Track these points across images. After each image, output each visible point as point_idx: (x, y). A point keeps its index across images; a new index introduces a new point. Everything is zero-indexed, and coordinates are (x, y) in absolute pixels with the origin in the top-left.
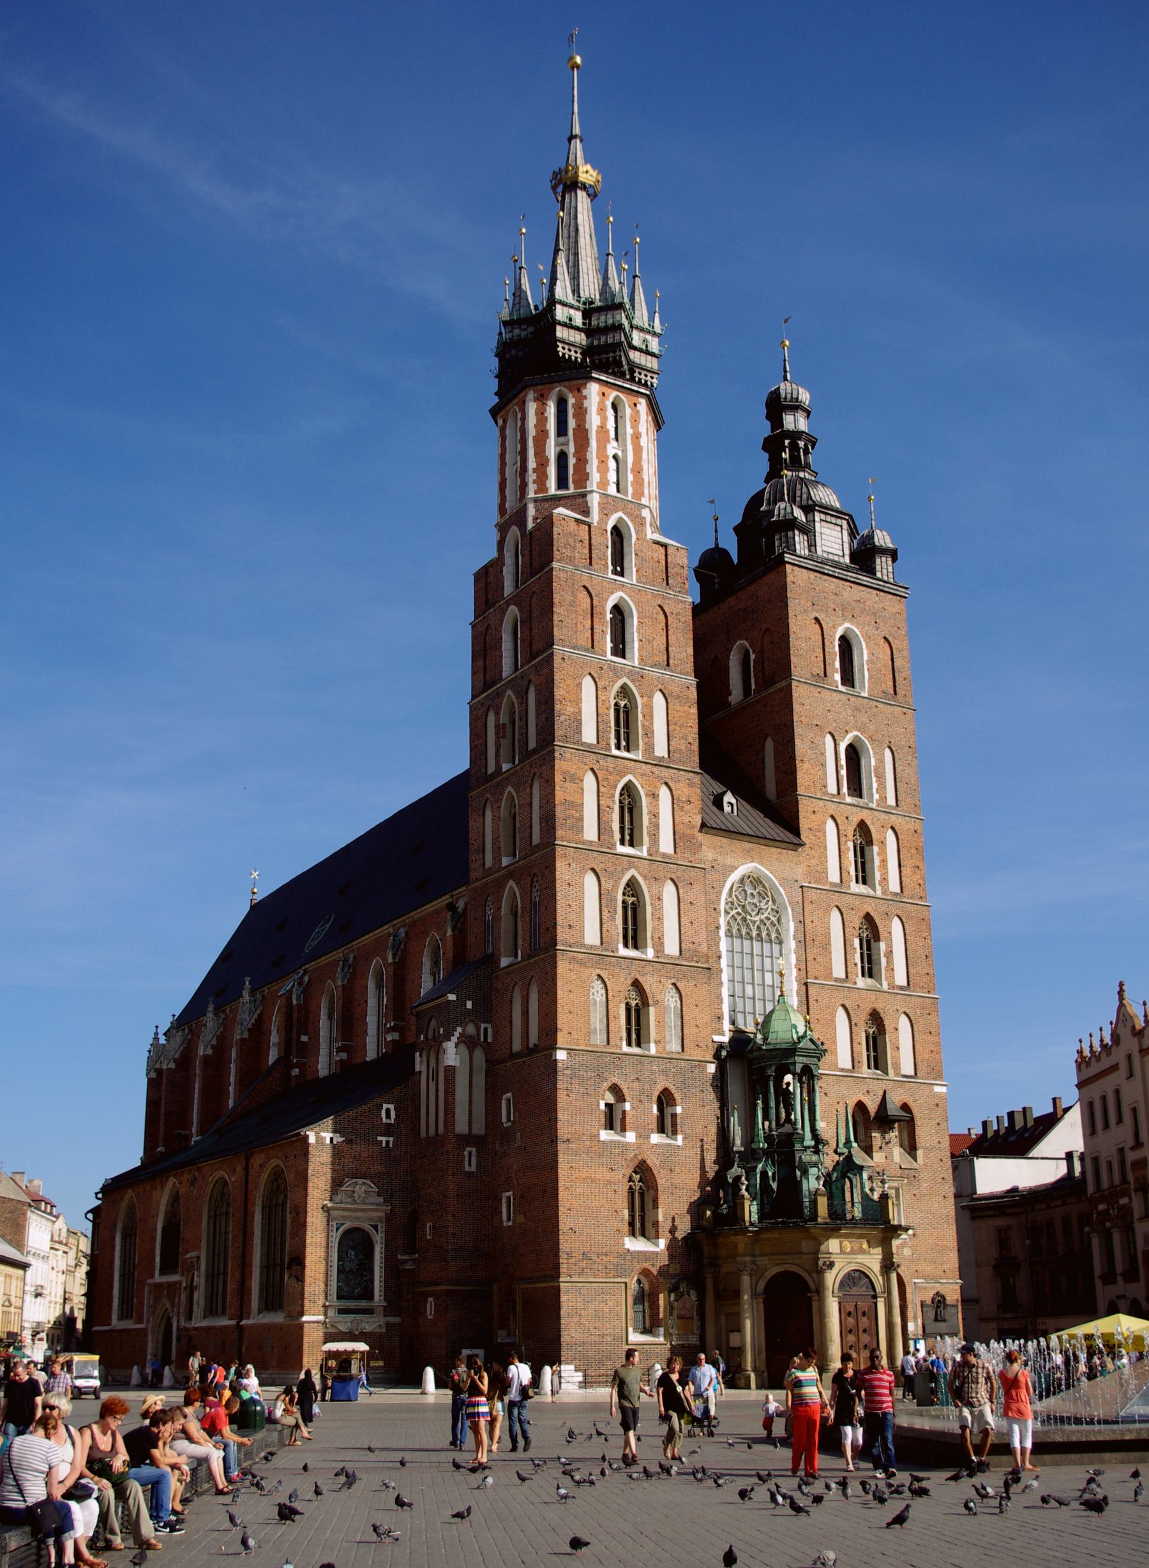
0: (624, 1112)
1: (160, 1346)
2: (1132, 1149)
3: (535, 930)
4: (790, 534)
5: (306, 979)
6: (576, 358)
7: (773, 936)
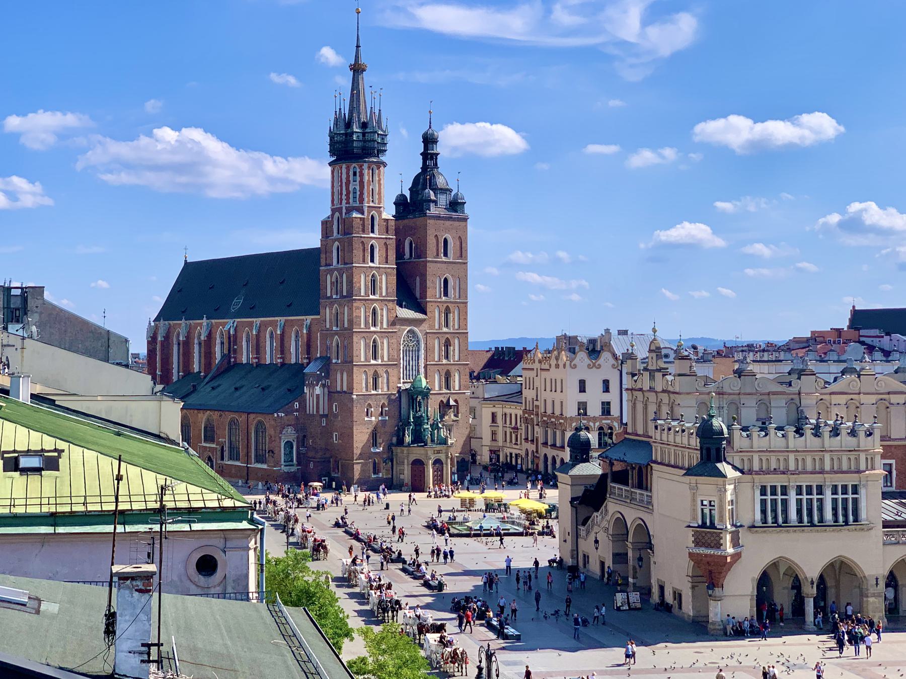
5: (235, 325)
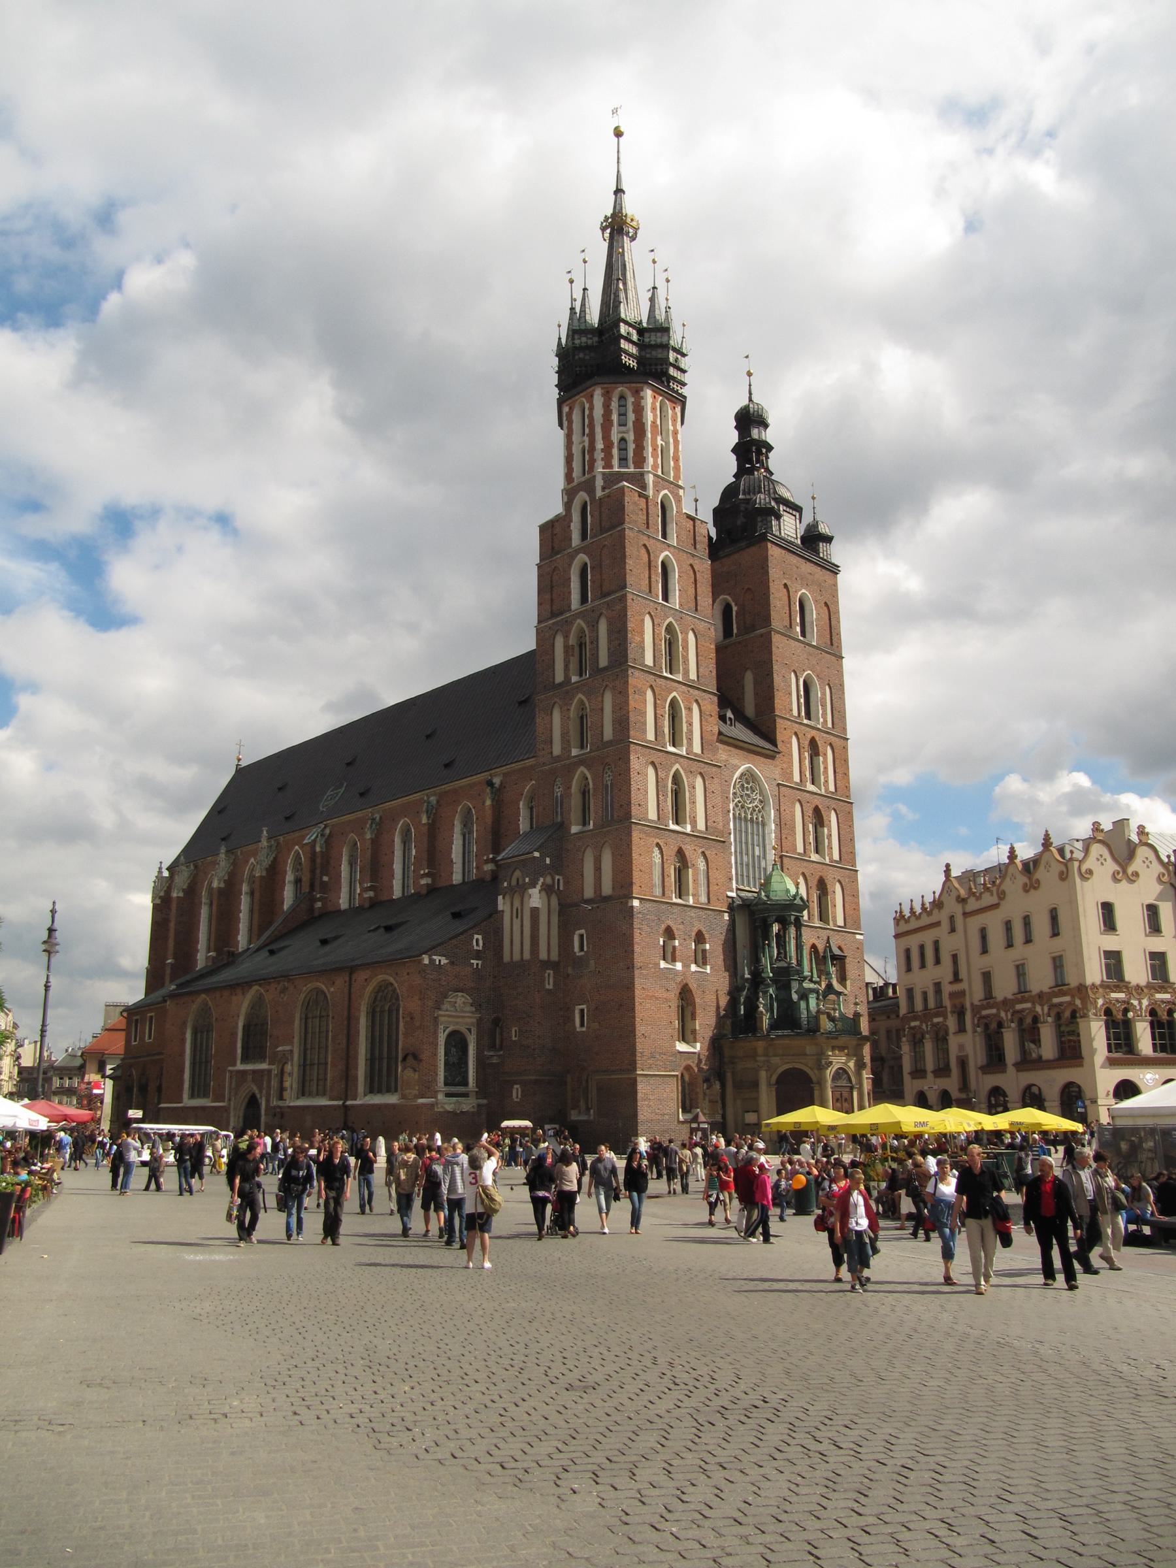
0: (674, 948)
1: (241, 1120)
2: (951, 983)
3: (607, 806)
4: (769, 518)
5: (327, 831)
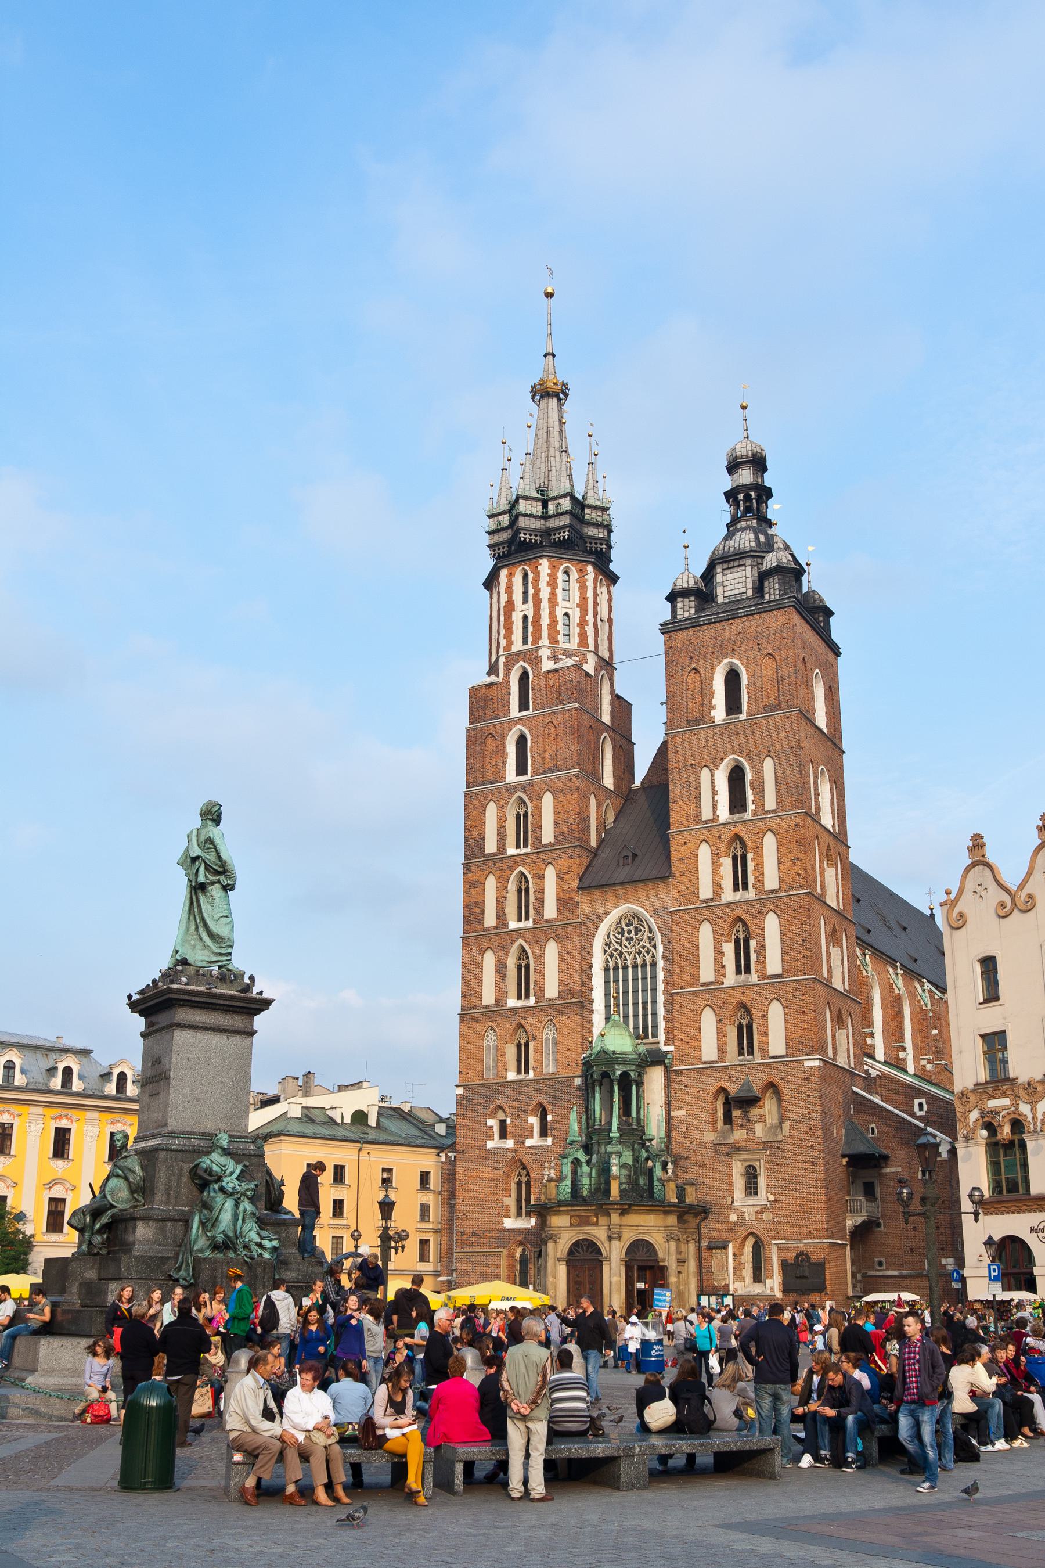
6: (503, 552)
7: (648, 959)
